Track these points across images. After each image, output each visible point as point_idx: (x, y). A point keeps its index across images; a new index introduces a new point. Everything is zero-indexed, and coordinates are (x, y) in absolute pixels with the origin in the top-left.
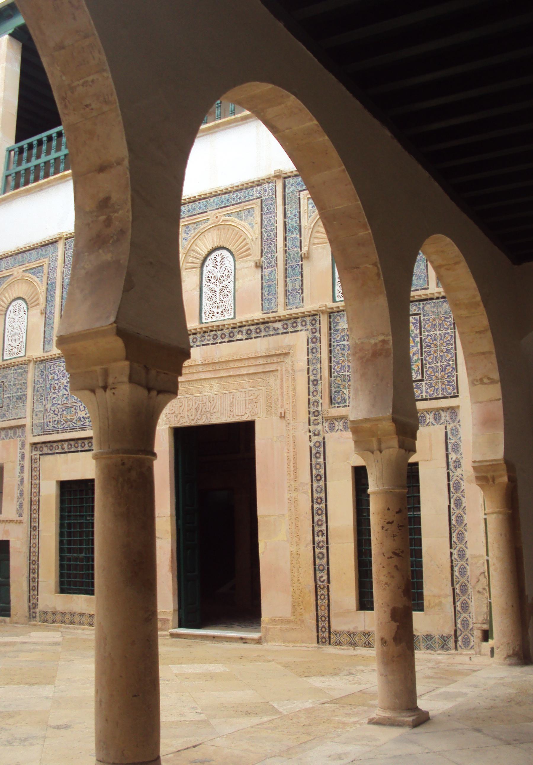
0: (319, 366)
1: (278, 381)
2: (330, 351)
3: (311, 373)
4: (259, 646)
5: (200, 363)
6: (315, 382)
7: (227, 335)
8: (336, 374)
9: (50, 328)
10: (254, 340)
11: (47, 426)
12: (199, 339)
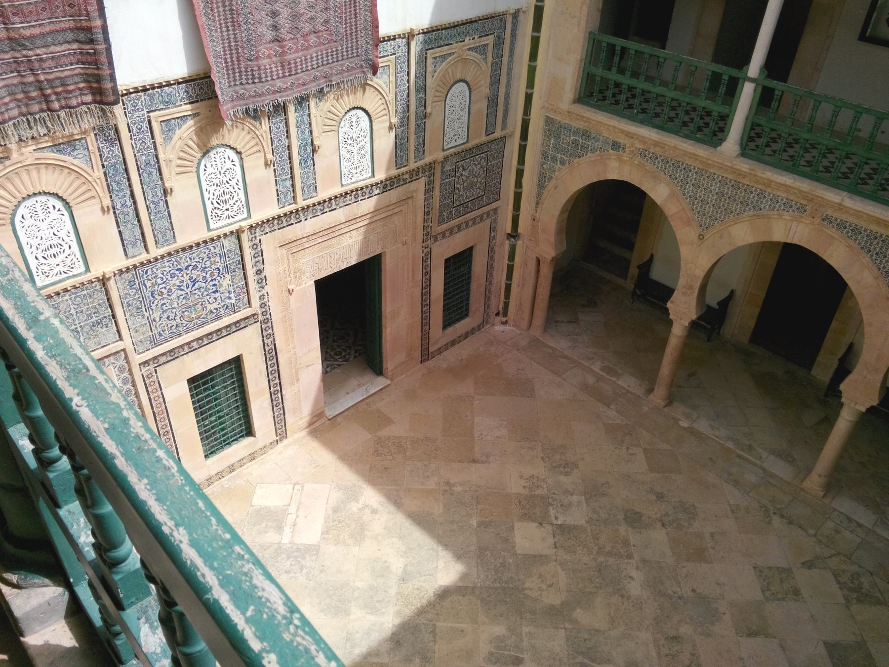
9: (129, 226)
11: (160, 335)
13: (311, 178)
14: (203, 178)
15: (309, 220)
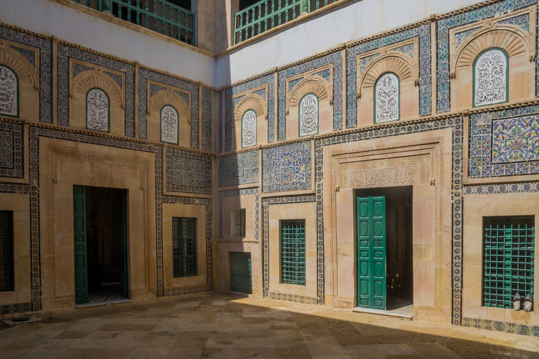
0: (461, 151)
1: (430, 161)
2: (469, 141)
3: (454, 155)
4: (411, 321)
5: (375, 149)
6: (458, 161)
7: (394, 131)
8: (473, 156)
10: (413, 134)
12: (374, 134)
13: (354, 115)
14: (301, 109)
15: (351, 142)
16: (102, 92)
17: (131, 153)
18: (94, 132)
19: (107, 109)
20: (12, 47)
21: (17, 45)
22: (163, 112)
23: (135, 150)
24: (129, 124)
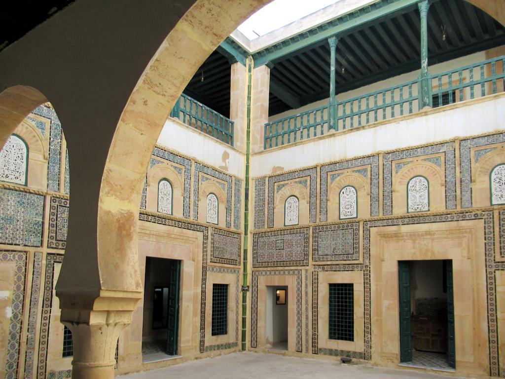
16: (421, 178)
17: (453, 224)
18: (416, 213)
19: (427, 191)
20: (353, 171)
21: (356, 169)
22: (493, 174)
23: (458, 220)
24: (451, 197)
